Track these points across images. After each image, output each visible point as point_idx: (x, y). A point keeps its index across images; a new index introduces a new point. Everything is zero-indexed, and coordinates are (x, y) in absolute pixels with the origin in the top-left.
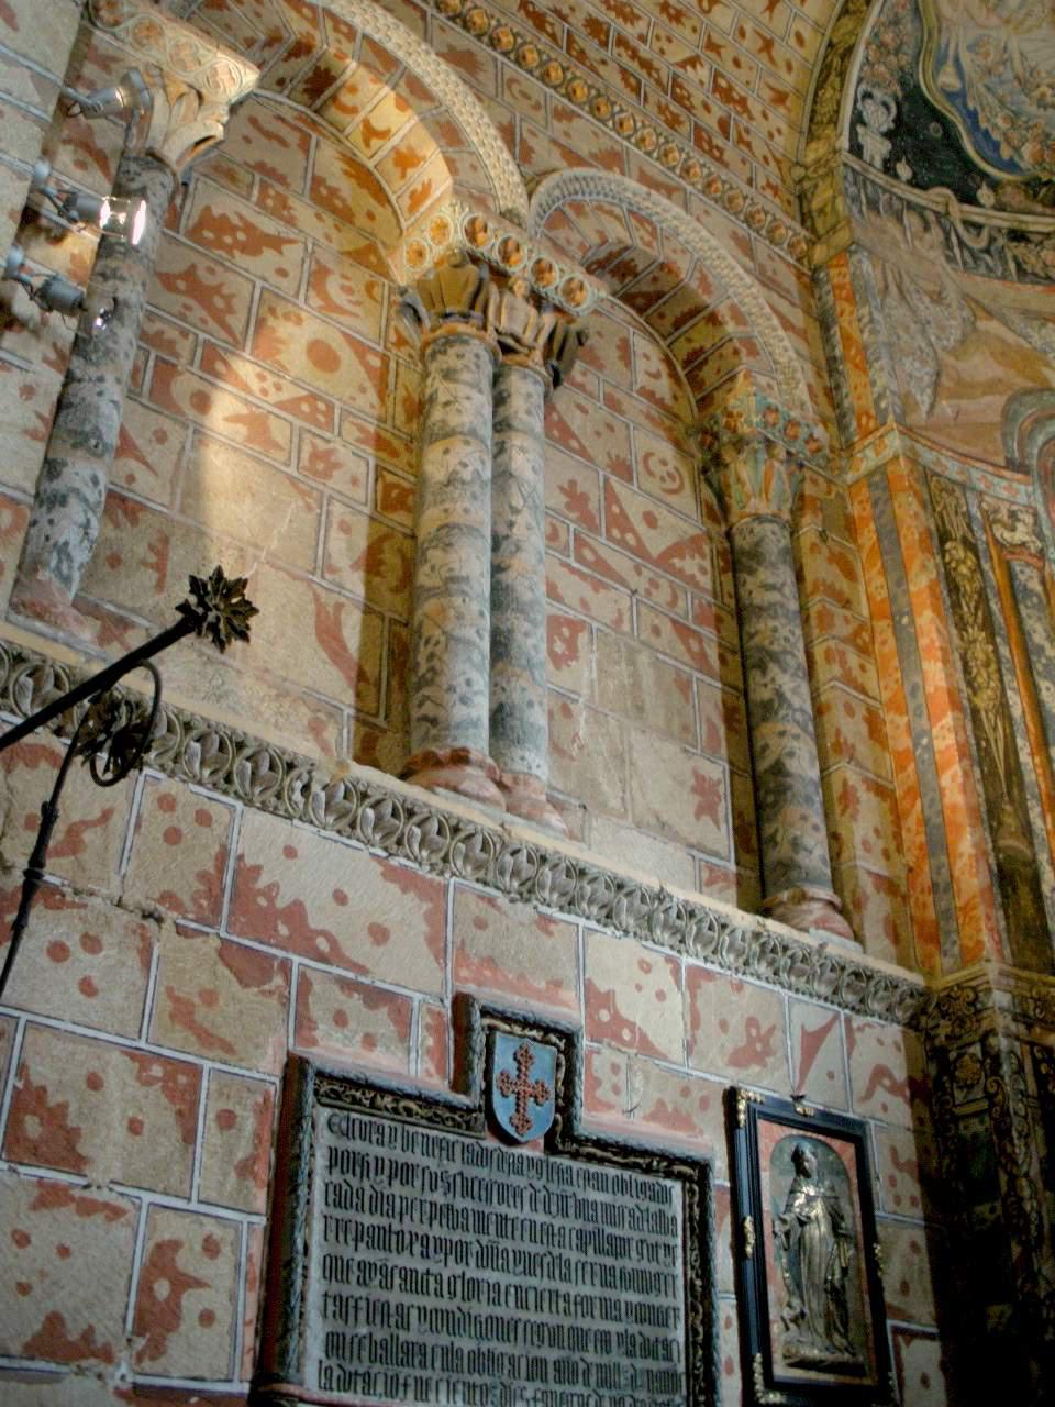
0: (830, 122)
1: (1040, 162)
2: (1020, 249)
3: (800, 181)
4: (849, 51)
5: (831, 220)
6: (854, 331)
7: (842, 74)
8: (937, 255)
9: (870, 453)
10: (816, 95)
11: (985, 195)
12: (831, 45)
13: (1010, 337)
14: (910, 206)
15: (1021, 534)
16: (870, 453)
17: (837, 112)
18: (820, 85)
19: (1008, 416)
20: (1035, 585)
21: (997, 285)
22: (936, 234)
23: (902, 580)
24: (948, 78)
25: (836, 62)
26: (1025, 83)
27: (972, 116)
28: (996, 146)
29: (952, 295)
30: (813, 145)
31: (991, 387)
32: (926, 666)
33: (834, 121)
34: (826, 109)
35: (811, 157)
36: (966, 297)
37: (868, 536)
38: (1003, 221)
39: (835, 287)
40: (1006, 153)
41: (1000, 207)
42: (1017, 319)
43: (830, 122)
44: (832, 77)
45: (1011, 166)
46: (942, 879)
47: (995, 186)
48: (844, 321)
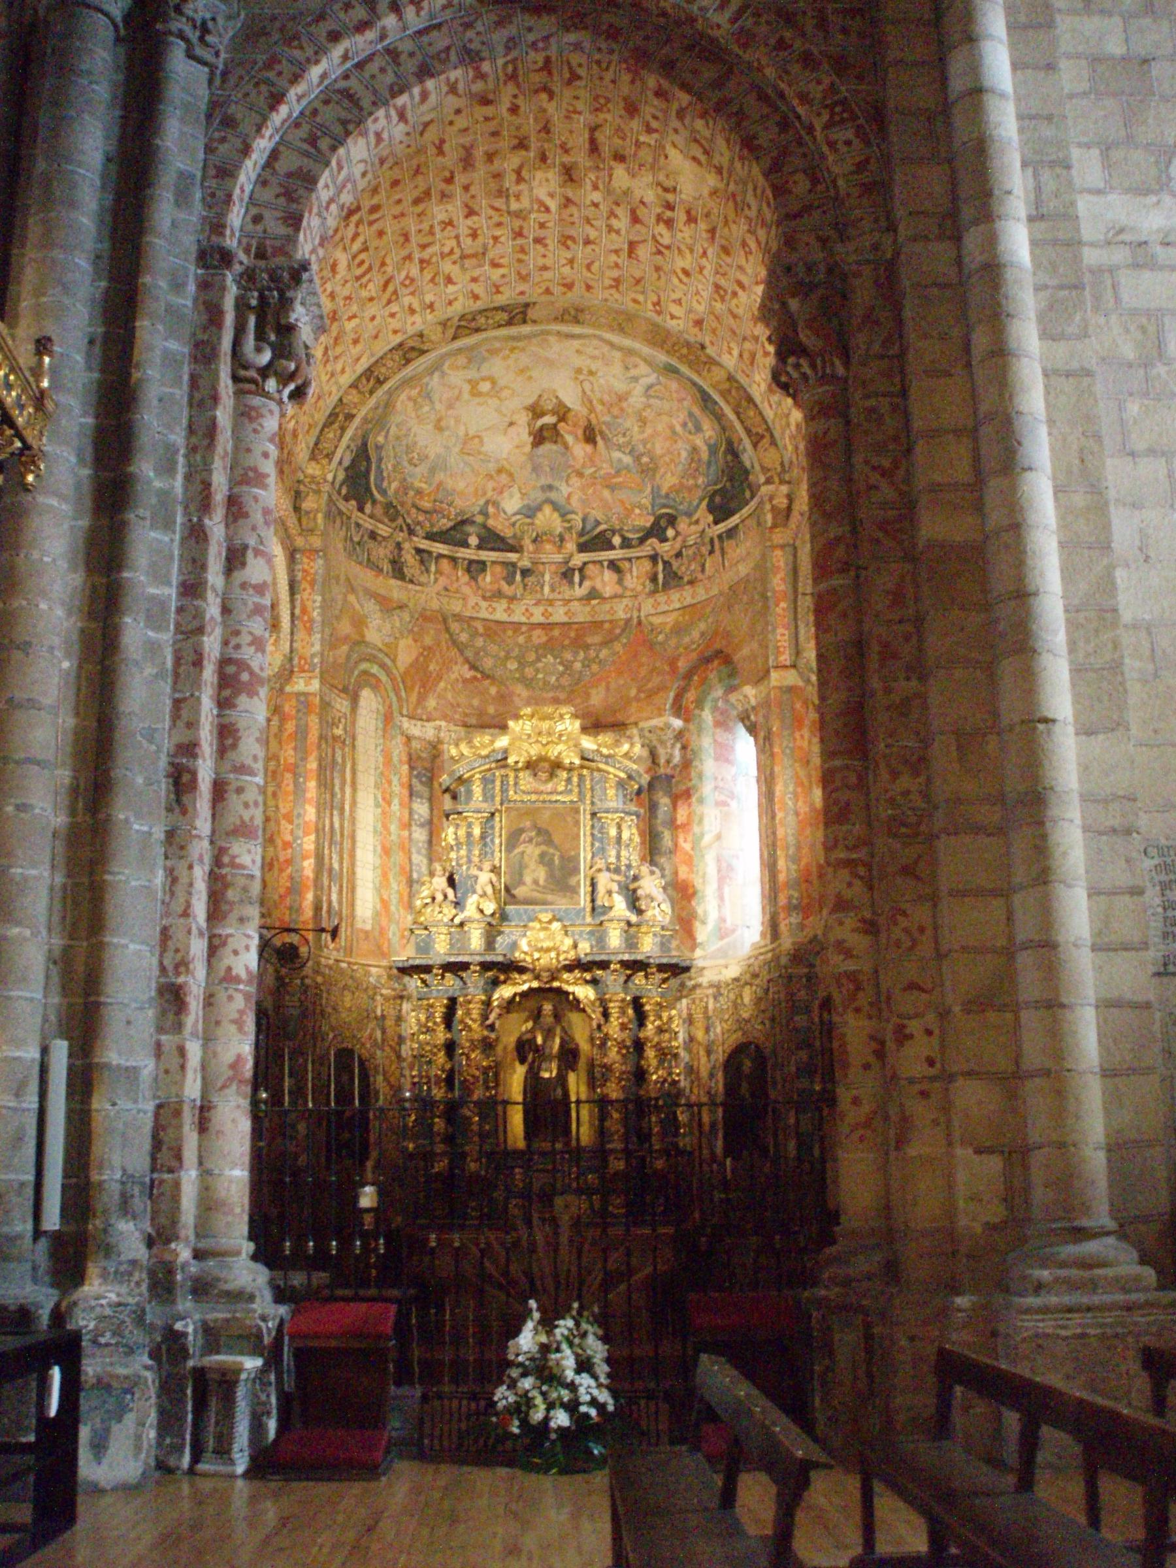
0: (327, 456)
1: (397, 491)
2: (371, 544)
3: (299, 482)
4: (350, 417)
5: (311, 525)
6: (309, 604)
7: (343, 429)
8: (340, 546)
9: (301, 681)
10: (322, 430)
11: (368, 508)
12: (341, 400)
13: (357, 606)
14: (341, 513)
15: (339, 732)
16: (301, 681)
17: (333, 453)
18: (327, 424)
19: (348, 657)
20: (340, 760)
21: (358, 568)
22: (342, 533)
23: (304, 759)
24: (381, 439)
25: (341, 417)
26: (409, 449)
27: (380, 460)
28: (383, 479)
29: (342, 578)
30: (313, 464)
31: (346, 638)
32: (307, 807)
33: (329, 456)
34: (326, 446)
35: (310, 471)
36: (348, 580)
37: (290, 727)
38: (368, 524)
39: (304, 571)
40: (385, 484)
41: (371, 516)
42: (361, 593)
43: (327, 456)
44: (336, 426)
45: (384, 492)
46: (296, 906)
47: (374, 502)
48: (305, 595)
